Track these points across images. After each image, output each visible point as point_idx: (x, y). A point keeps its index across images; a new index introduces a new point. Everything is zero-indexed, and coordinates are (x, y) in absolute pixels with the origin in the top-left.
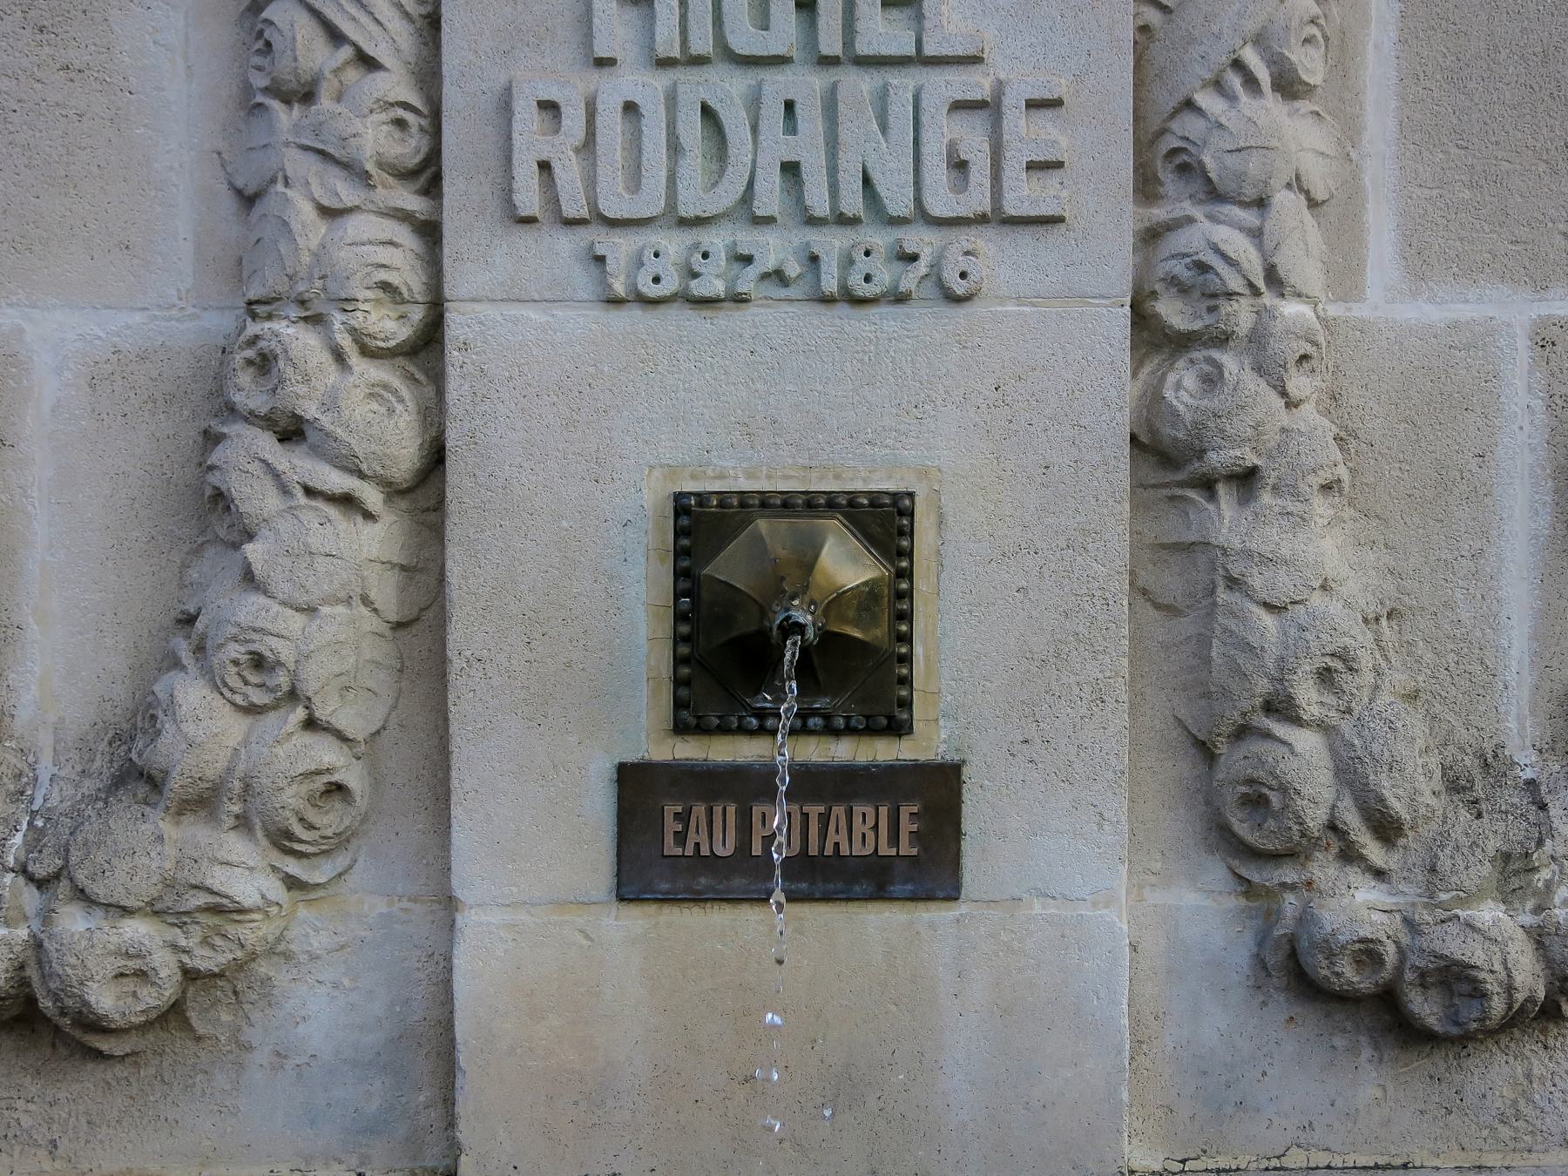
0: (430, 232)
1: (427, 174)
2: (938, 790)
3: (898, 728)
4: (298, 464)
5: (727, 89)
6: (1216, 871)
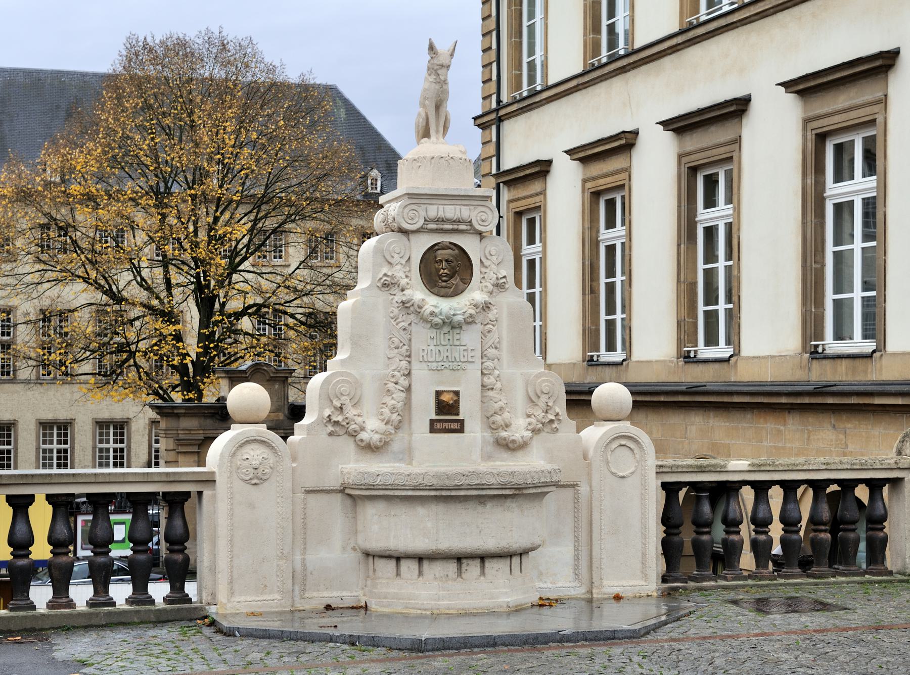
0: (410, 362)
1: (409, 356)
2: (462, 422)
3: (458, 415)
4: (397, 386)
5: (441, 348)
6: (489, 431)
